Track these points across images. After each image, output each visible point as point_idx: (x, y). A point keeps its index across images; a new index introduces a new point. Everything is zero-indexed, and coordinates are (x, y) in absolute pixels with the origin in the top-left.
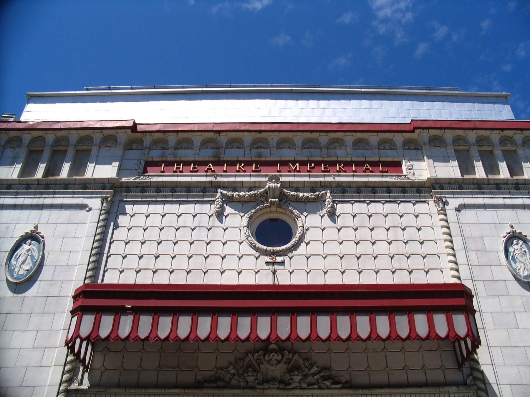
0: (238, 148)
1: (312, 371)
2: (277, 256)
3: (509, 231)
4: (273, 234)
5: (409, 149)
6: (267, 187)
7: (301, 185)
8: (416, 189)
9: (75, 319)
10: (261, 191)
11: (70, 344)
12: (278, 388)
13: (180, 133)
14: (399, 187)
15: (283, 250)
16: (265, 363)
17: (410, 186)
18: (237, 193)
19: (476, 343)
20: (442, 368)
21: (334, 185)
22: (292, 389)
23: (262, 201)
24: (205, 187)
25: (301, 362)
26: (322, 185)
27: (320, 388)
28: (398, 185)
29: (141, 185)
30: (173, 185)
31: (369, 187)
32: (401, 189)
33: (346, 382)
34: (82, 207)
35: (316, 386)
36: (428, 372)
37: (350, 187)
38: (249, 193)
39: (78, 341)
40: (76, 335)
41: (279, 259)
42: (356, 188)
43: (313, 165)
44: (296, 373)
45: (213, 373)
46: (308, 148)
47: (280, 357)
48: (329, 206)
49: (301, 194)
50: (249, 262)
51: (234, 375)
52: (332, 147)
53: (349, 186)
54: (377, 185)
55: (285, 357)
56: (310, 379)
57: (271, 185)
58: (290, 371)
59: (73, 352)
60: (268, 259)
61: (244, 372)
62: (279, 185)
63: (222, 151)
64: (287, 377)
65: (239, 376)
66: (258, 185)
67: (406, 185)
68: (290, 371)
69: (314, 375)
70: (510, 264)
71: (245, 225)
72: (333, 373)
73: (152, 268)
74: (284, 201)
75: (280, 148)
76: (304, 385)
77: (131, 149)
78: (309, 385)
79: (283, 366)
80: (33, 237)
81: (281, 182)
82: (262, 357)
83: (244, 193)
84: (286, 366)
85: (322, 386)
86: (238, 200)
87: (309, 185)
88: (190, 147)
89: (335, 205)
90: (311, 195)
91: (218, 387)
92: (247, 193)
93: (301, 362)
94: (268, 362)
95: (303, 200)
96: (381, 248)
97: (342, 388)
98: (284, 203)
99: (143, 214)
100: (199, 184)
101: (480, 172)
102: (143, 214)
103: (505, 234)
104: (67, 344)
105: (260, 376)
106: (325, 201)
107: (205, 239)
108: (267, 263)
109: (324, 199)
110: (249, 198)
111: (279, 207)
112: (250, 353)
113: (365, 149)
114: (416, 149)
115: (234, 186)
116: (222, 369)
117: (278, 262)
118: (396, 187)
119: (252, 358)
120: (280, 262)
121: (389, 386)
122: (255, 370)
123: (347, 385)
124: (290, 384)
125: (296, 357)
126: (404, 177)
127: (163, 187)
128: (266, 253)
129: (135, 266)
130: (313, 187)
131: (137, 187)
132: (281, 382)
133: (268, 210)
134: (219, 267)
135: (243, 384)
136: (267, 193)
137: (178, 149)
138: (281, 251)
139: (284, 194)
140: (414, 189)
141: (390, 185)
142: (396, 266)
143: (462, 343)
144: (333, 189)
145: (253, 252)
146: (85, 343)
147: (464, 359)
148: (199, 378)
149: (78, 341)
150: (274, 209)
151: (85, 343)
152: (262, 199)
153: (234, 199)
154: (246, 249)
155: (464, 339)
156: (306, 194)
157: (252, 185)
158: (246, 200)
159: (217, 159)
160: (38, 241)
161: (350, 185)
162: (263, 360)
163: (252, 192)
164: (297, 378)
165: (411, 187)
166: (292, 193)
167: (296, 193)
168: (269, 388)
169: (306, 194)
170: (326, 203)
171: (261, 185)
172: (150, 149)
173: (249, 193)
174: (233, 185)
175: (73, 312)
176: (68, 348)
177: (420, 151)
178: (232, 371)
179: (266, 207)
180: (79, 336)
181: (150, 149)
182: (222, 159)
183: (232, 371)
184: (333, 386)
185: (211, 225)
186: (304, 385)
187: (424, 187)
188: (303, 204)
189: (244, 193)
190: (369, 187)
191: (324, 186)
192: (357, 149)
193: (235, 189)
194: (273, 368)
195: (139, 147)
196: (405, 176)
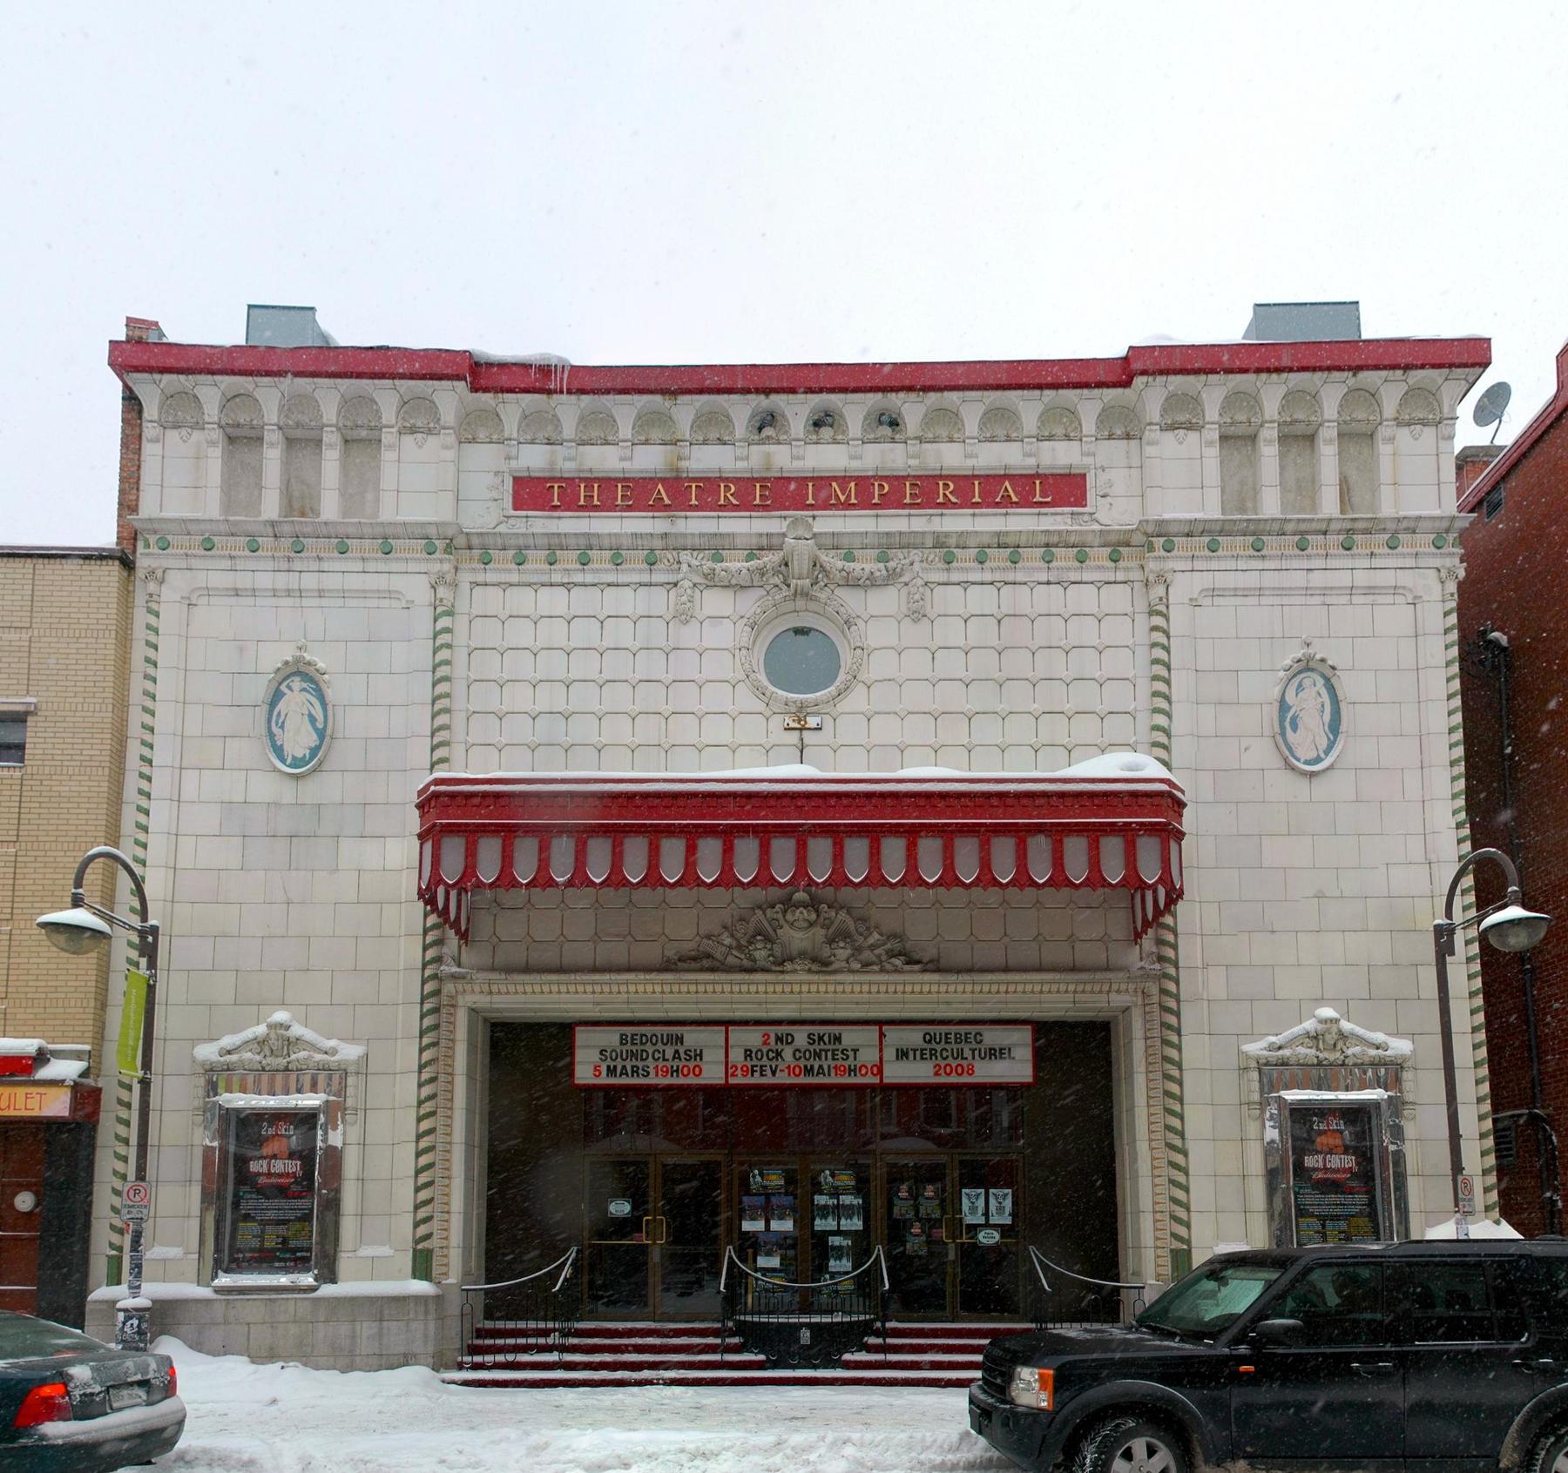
1: (871, 941)
3: (1299, 655)
4: (802, 659)
9: (428, 846)
11: (427, 896)
12: (810, 971)
16: (786, 926)
19: (1175, 895)
20: (1104, 940)
22: (835, 972)
25: (852, 928)
27: (882, 971)
29: (513, 542)
33: (931, 961)
34: (390, 594)
35: (876, 968)
36: (1078, 945)
39: (441, 890)
40: (436, 880)
44: (842, 944)
45: (693, 945)
47: (813, 916)
51: (730, 947)
55: (823, 915)
58: (831, 941)
59: (435, 909)
61: (750, 943)
64: (826, 952)
65: (739, 947)
68: (831, 941)
69: (872, 947)
70: (1283, 734)
72: (908, 945)
78: (866, 964)
79: (819, 933)
82: (780, 916)
84: (823, 932)
85: (888, 967)
91: (702, 970)
97: (924, 971)
103: (1288, 662)
104: (421, 894)
105: (777, 950)
112: (760, 907)
116: (709, 937)
119: (762, 917)
123: (930, 966)
124: (830, 963)
130: (887, 545)
132: (814, 960)
135: (746, 963)
143: (1149, 895)
146: (453, 893)
147: (1147, 924)
148: (670, 953)
149: (441, 890)
151: (453, 893)
152: (777, 580)
154: (747, 699)
155: (1154, 888)
160: (312, 680)
162: (782, 922)
164: (843, 953)
168: (794, 971)
175: (422, 837)
176: (426, 903)
178: (728, 941)
180: (441, 881)
183: (728, 941)
184: (907, 967)
187: (1128, 545)
188: (861, 592)
191: (907, 542)
194: (800, 935)
195: (495, 437)
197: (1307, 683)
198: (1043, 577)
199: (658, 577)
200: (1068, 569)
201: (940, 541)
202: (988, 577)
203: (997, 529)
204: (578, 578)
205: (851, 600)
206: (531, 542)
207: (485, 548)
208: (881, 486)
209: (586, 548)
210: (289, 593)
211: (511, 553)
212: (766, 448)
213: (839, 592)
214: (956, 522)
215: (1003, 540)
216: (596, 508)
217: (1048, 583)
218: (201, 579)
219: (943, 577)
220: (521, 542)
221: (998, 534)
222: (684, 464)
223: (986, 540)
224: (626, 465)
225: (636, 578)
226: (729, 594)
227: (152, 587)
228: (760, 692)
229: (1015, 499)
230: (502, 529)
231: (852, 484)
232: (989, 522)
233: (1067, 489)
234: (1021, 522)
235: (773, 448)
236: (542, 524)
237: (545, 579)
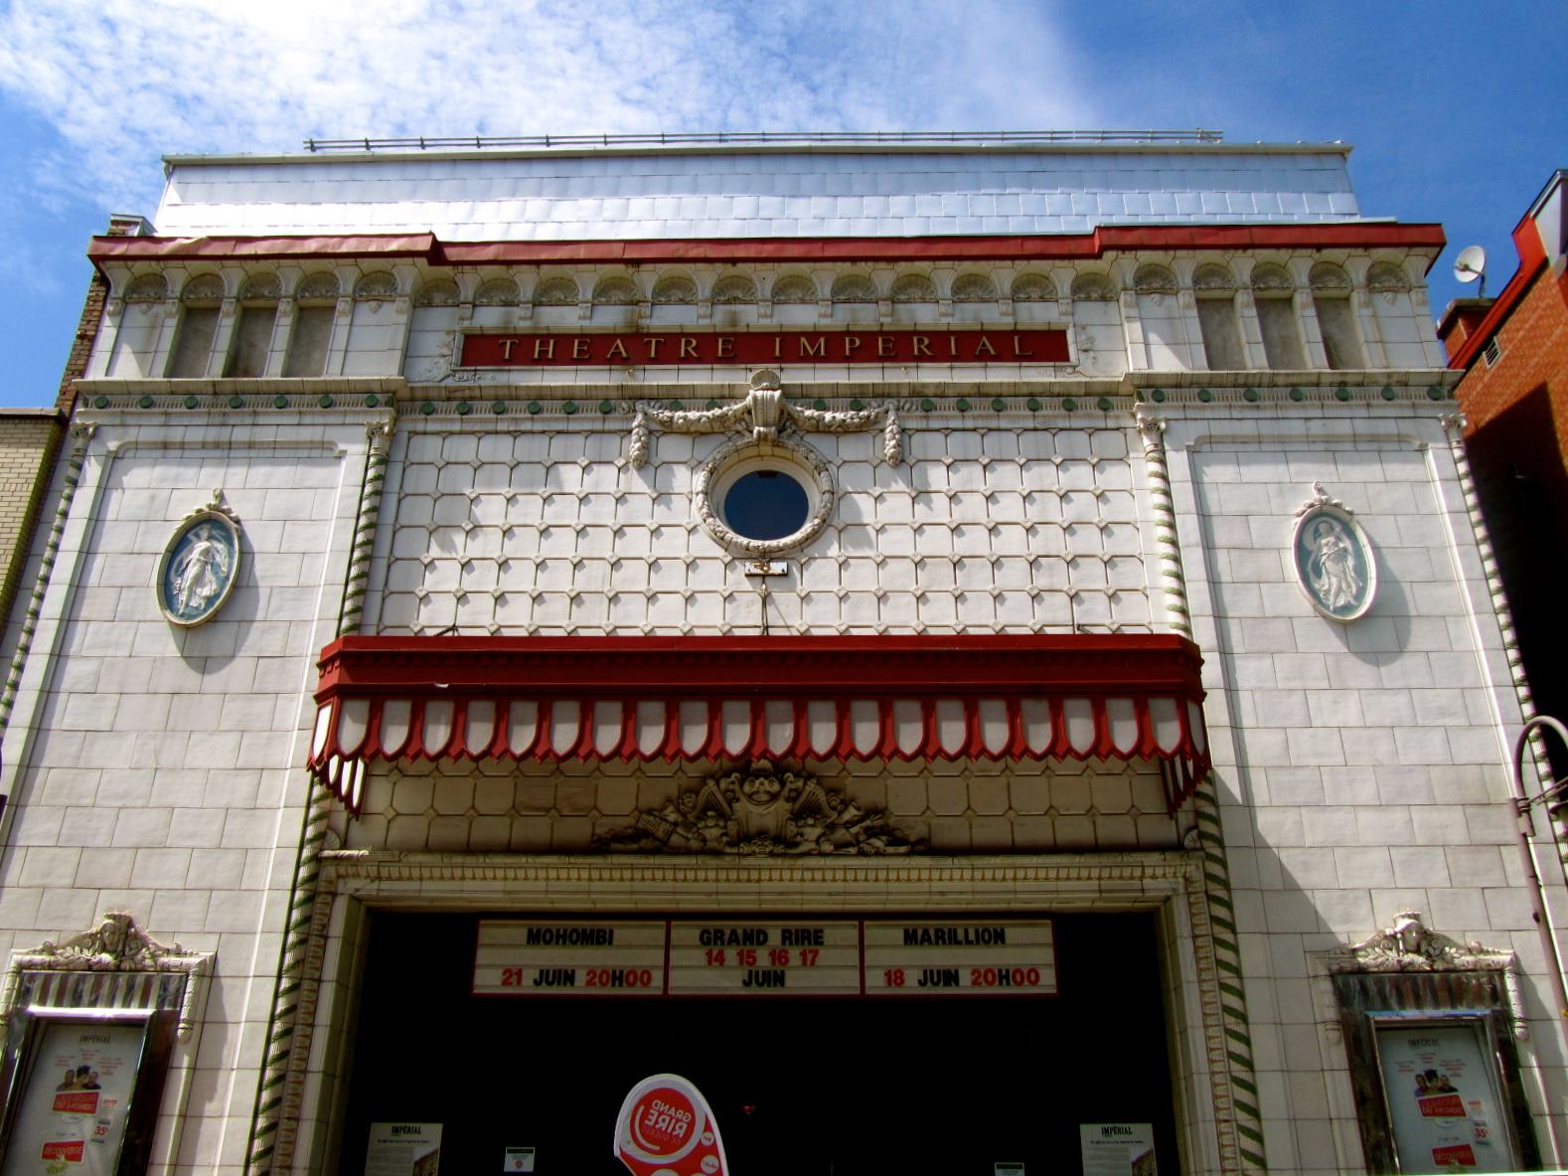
0: (683, 302)
1: (846, 817)
2: (772, 560)
4: (763, 506)
5: (1088, 299)
6: (749, 398)
7: (827, 392)
8: (1097, 399)
10: (735, 407)
11: (318, 769)
12: (772, 854)
13: (545, 268)
14: (1058, 395)
15: (786, 545)
16: (743, 798)
17: (1082, 392)
18: (681, 413)
21: (905, 392)
23: (738, 432)
24: (607, 400)
25: (822, 797)
26: (879, 391)
27: (862, 853)
28: (1056, 390)
29: (458, 394)
30: (533, 394)
31: (987, 395)
32: (1061, 399)
33: (921, 841)
35: (853, 850)
36: (1100, 820)
37: (942, 396)
38: (710, 414)
39: (334, 761)
40: (333, 746)
41: (777, 567)
42: (956, 399)
43: (858, 342)
44: (810, 821)
45: (631, 821)
46: (845, 302)
47: (776, 787)
48: (893, 442)
49: (828, 416)
50: (711, 575)
51: (675, 824)
52: (902, 297)
53: (939, 392)
54: (1005, 391)
55: (789, 786)
56: (841, 834)
57: (759, 393)
60: (751, 567)
61: (699, 818)
62: (777, 394)
63: (646, 309)
64: (792, 829)
65: (689, 826)
66: (729, 395)
67: (1074, 390)
68: (797, 816)
71: (700, 489)
72: (892, 821)
73: (491, 590)
74: (789, 431)
75: (780, 303)
76: (827, 847)
77: (430, 305)
78: (839, 846)
79: (782, 807)
80: (213, 522)
81: (782, 387)
82: (736, 787)
83: (698, 414)
84: (788, 806)
85: (867, 848)
86: (684, 429)
87: (848, 392)
88: (569, 300)
89: (907, 438)
90: (852, 418)
91: (641, 852)
92: (705, 413)
93: (822, 797)
94: (750, 797)
95: (832, 429)
96: (1012, 540)
97: (907, 854)
98: (789, 436)
99: (468, 463)
100: (594, 393)
101: (1255, 360)
102: (468, 463)
103: (1300, 509)
105: (732, 827)
106: (882, 431)
107: (610, 521)
108: (749, 576)
109: (880, 427)
110: (708, 425)
111: (778, 446)
112: (712, 777)
113: (983, 301)
114: (1103, 299)
115: (675, 398)
116: (650, 812)
117: (773, 575)
118: (1052, 395)
120: (779, 575)
121: (1013, 850)
122: (722, 815)
123: (921, 848)
124: (797, 844)
125: (812, 785)
126: (1070, 370)
127: (511, 399)
128: (747, 554)
129: (454, 586)
130: (857, 397)
131: (449, 399)
132: (778, 839)
133: (754, 451)
134: (643, 587)
135: (694, 844)
136: (749, 412)
137: (541, 304)
138: (781, 549)
139: (790, 417)
140: (1094, 400)
141: (1038, 390)
142: (1042, 581)
144: (903, 401)
145: (720, 552)
146: (348, 766)
147: (1180, 796)
148: (600, 831)
149: (334, 761)
150: (766, 449)
151: (348, 766)
153: (674, 426)
154: (703, 544)
156: (840, 416)
157: (716, 393)
158: (702, 429)
159: (634, 330)
161: (942, 391)
162: (739, 794)
163: (717, 412)
164: (813, 833)
165: (1086, 395)
166: (808, 413)
167: (816, 413)
168: (753, 854)
169: (840, 416)
170: (888, 436)
171: (737, 392)
172: (475, 306)
173: (710, 414)
174: (673, 392)
175: (321, 698)
176: (315, 774)
177: (1112, 305)
179: (748, 445)
181: (475, 306)
182: (645, 331)
183: (673, 817)
184: (890, 850)
185: (623, 488)
186: (827, 847)
189: (698, 414)
190: (987, 395)
191: (881, 393)
192: (962, 301)
193: (676, 405)
194: (761, 810)
195: (450, 301)
196: (1075, 367)
197: (1322, 528)
198: (1030, 424)
199: (610, 426)
200: (1055, 417)
201: (917, 393)
202: (970, 424)
203: (977, 381)
204: (527, 426)
205: (823, 445)
206: (477, 393)
207: (427, 399)
208: (852, 342)
209: (536, 401)
210: (217, 445)
211: (455, 404)
212: (732, 307)
213: (809, 438)
214: (932, 375)
215: (984, 390)
216: (554, 362)
217: (1035, 430)
218: (132, 435)
219: (922, 425)
220: (467, 393)
221: (979, 385)
222: (645, 322)
223: (966, 391)
224: (586, 323)
225: (588, 426)
226: (687, 441)
227: (80, 443)
228: (720, 540)
229: (992, 352)
230: (450, 382)
231: (822, 340)
232: (968, 375)
233: (1049, 346)
234: (1001, 375)
235: (740, 308)
236: (491, 378)
237: (491, 427)
